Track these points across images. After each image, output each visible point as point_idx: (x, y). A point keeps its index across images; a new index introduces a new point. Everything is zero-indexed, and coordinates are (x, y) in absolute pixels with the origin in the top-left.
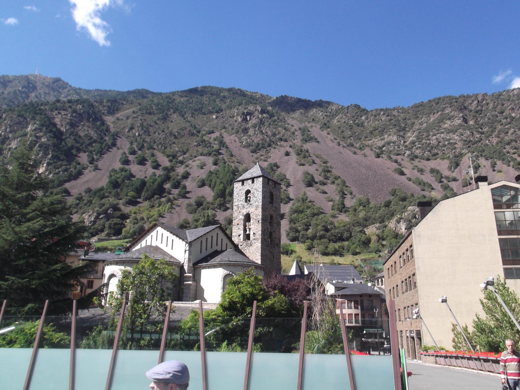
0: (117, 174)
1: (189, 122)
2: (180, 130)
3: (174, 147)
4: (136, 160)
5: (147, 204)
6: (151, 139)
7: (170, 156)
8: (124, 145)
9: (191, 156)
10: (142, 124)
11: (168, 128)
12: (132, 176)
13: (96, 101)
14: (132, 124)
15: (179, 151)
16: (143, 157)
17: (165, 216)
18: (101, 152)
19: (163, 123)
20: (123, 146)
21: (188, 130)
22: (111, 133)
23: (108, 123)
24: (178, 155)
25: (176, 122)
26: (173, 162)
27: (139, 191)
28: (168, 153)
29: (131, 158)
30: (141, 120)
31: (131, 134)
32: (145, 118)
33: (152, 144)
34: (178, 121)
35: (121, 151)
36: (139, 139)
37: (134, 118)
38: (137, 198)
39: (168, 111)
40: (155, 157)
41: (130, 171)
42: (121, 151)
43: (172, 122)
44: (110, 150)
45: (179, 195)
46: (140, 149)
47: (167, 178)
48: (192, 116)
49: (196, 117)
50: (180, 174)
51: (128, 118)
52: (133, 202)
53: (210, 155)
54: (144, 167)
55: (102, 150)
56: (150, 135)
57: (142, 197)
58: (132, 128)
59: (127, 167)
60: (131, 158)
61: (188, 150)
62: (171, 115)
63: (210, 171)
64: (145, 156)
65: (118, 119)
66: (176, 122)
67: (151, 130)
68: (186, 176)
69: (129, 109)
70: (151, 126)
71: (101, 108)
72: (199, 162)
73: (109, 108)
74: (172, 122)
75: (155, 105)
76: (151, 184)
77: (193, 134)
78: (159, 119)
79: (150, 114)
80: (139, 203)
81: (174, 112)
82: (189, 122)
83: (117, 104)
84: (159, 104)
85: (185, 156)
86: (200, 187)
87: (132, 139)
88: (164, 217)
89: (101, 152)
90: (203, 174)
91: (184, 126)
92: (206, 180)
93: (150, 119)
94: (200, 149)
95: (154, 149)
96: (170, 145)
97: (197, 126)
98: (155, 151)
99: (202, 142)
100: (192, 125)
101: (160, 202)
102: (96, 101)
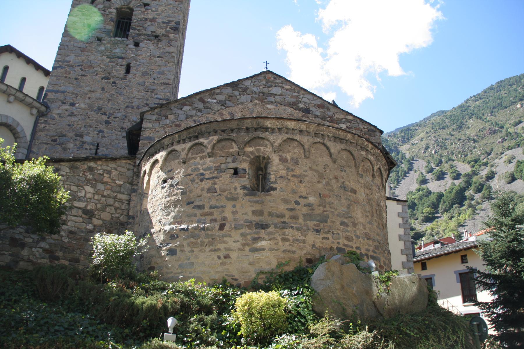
0: (414, 195)
1: (489, 121)
2: (479, 132)
3: (475, 152)
4: (433, 176)
5: (445, 216)
6: (448, 152)
7: (472, 161)
8: (421, 166)
9: (497, 153)
10: (437, 140)
11: (465, 135)
12: (429, 193)
13: (390, 136)
14: (427, 144)
15: (482, 154)
16: (440, 171)
17: (466, 224)
18: (398, 179)
19: (460, 132)
20: (420, 168)
21: (488, 129)
22: (406, 160)
23: (403, 151)
24: (481, 158)
25: (473, 127)
26: (476, 167)
27: (435, 206)
28: (469, 159)
29: (429, 176)
30: (435, 137)
31: (427, 154)
32: (438, 134)
33: (450, 156)
34: (475, 125)
35: (418, 173)
36: (436, 156)
37: (427, 138)
38: (434, 213)
39: (463, 119)
40: (455, 168)
41: (428, 189)
42: (418, 173)
43: (469, 128)
44: (407, 175)
45: (484, 197)
46: (438, 165)
47: (469, 184)
48: (492, 115)
49: (497, 114)
50: (484, 176)
51: (422, 140)
52: (429, 219)
53: (519, 145)
54: (444, 181)
55: (399, 177)
56: (446, 149)
57: (440, 212)
58: (427, 148)
59: (424, 186)
60: (429, 176)
61: (492, 150)
62: (467, 121)
63: (519, 161)
64: (444, 170)
65: (413, 145)
66: (473, 127)
67: (448, 143)
68: (491, 177)
69: (423, 132)
70: (446, 139)
71: (395, 140)
72: (506, 157)
73: (403, 137)
74: (469, 128)
75: (447, 118)
76: (448, 194)
77: (495, 132)
78: (453, 130)
79: (443, 128)
80: (438, 217)
81: (470, 118)
82: (489, 121)
83: (410, 132)
84: (451, 116)
85: (489, 157)
86: (509, 183)
87: (429, 158)
88: (465, 226)
89: (398, 179)
90: (511, 168)
91: (482, 127)
92: (515, 173)
93: (444, 134)
94: (506, 144)
95: (453, 160)
96: (471, 151)
97: (499, 123)
98: (455, 162)
99: (507, 136)
100: (492, 123)
101: (459, 210)
102: (390, 136)
